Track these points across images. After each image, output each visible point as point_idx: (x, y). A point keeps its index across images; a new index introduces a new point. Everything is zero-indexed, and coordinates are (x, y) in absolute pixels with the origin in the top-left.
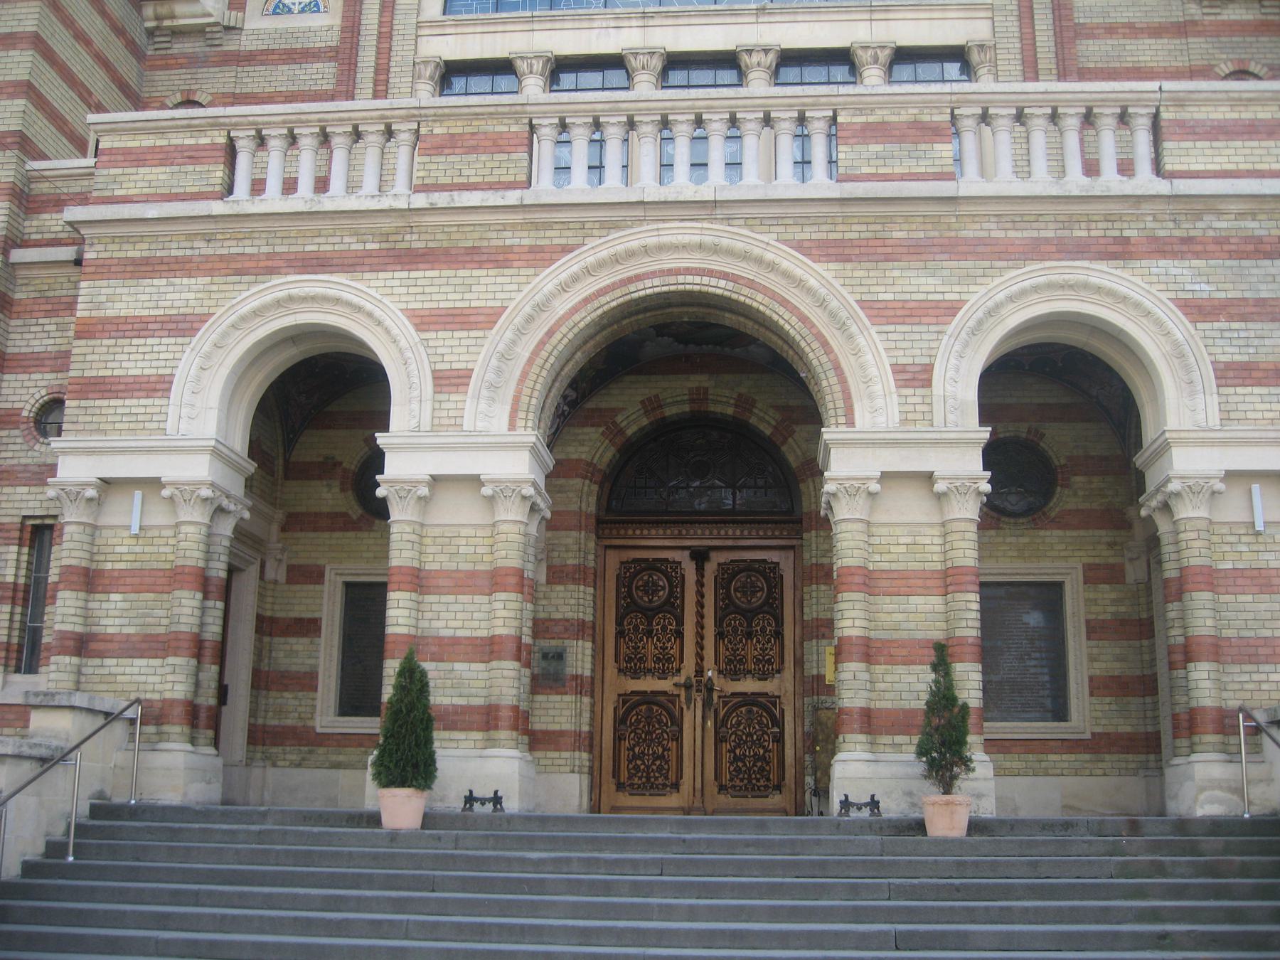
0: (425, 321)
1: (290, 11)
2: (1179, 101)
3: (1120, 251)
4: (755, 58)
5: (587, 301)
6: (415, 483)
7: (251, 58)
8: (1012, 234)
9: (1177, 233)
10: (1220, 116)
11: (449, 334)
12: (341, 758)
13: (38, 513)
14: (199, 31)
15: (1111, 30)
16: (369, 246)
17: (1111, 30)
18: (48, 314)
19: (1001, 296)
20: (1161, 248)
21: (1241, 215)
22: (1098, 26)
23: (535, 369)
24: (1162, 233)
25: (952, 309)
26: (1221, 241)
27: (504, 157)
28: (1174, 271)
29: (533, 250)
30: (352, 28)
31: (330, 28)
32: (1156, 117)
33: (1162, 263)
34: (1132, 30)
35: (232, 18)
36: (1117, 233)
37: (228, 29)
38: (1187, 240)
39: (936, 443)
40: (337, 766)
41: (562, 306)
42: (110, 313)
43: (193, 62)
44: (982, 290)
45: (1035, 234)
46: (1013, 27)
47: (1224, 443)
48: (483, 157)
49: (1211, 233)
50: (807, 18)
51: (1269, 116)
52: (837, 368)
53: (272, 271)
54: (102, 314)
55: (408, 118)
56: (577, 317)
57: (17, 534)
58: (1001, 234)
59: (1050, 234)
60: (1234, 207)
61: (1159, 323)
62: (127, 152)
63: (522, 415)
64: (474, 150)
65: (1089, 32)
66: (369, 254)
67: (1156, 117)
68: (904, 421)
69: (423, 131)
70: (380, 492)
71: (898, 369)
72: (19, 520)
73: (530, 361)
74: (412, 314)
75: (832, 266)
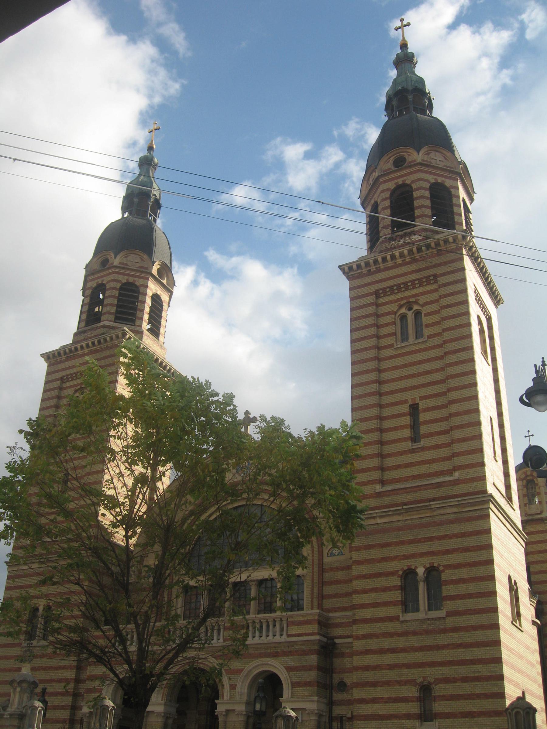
2: (291, 616)
3: (276, 655)
8: (256, 652)
9: (288, 650)
10: (300, 619)
15: (332, 569)
20: (285, 654)
21: (301, 645)
24: (285, 650)
28: (286, 659)
33: (284, 658)
34: (337, 569)
36: (276, 651)
38: (290, 652)
39: (236, 703)
44: (247, 666)
45: (260, 652)
47: (292, 702)
49: (295, 650)
50: (264, 570)
51: (310, 619)
54: (91, 674)
57: (79, 722)
58: (253, 652)
59: (263, 651)
60: (300, 643)
63: (164, 697)
68: (230, 698)
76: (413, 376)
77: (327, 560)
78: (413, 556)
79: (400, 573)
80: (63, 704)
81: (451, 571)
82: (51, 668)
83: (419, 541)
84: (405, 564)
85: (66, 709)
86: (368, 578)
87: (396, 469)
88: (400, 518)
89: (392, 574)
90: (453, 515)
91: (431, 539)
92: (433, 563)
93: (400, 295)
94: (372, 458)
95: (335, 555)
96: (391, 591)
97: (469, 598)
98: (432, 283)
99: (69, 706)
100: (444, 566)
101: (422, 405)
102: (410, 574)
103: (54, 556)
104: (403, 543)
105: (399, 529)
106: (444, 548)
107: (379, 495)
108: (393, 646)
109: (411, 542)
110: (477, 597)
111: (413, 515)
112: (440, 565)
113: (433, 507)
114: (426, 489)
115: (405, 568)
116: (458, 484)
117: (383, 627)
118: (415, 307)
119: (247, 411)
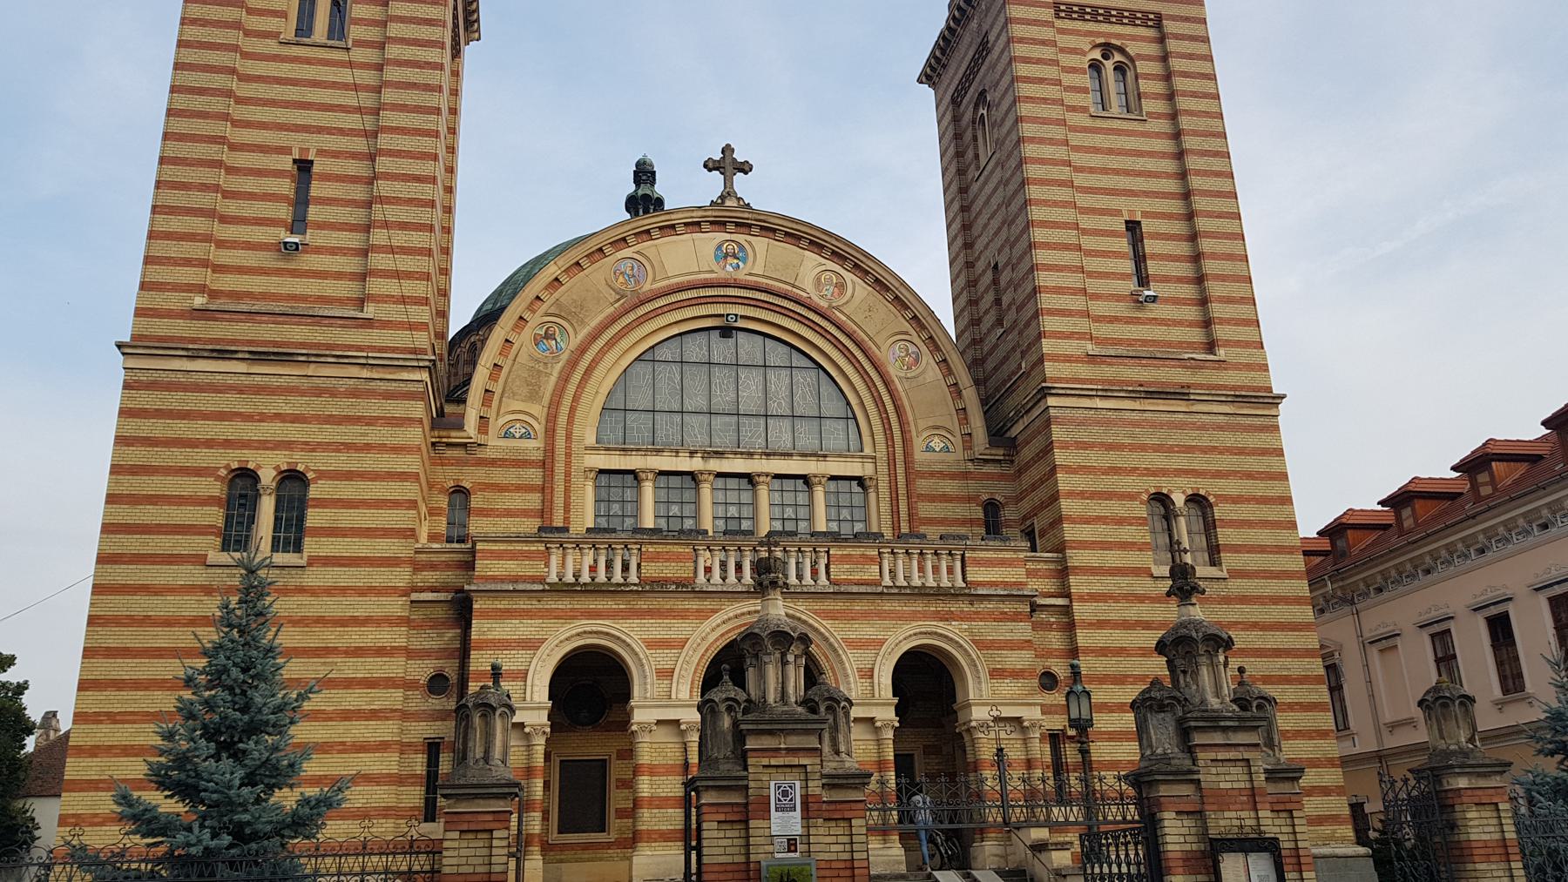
0: (652, 644)
1: (514, 437)
4: (762, 479)
5: (722, 635)
6: (649, 724)
7: (493, 463)
11: (661, 651)
12: (562, 857)
13: (432, 736)
14: (464, 445)
15: (932, 474)
16: (621, 607)
17: (932, 474)
18: (431, 628)
19: (901, 638)
22: (926, 472)
23: (701, 668)
25: (882, 643)
26: (991, 613)
27: (682, 564)
29: (698, 611)
30: (550, 450)
31: (539, 449)
32: (963, 556)
34: (942, 475)
35: (481, 439)
37: (479, 445)
39: (877, 704)
40: (561, 861)
41: (711, 638)
42: (490, 637)
43: (459, 462)
46: (883, 468)
48: (673, 564)
52: (832, 668)
53: (574, 618)
55: (636, 543)
56: (718, 643)
61: (965, 650)
62: (492, 552)
64: (667, 560)
65: (922, 475)
66: (621, 611)
67: (963, 556)
69: (643, 549)
70: (634, 728)
71: (860, 670)
72: (421, 740)
73: (698, 664)
74: (644, 641)
75: (830, 622)
76: (1127, 173)
77: (919, 456)
78: (1164, 472)
79: (1145, 497)
80: (372, 707)
81: (1228, 506)
82: (320, 621)
83: (1171, 449)
84: (1152, 485)
85: (387, 719)
86: (1087, 498)
87: (1111, 322)
88: (1136, 405)
89: (1131, 497)
90: (1221, 417)
91: (1189, 449)
92: (1198, 488)
93: (1105, 28)
94: (1072, 294)
95: (934, 451)
96: (1131, 524)
97: (1259, 552)
98: (1151, 26)
99: (396, 710)
100: (1215, 496)
101: (1147, 226)
102: (1161, 499)
103: (240, 348)
104: (1143, 448)
105: (1135, 424)
106: (1213, 468)
107: (1092, 359)
108: (1146, 617)
109: (1158, 449)
110: (1271, 552)
111: (1158, 404)
112: (1210, 494)
113: (1192, 397)
114: (1174, 367)
115: (1153, 491)
116: (1225, 369)
117: (1124, 584)
118: (1118, 57)
119: (728, 146)
